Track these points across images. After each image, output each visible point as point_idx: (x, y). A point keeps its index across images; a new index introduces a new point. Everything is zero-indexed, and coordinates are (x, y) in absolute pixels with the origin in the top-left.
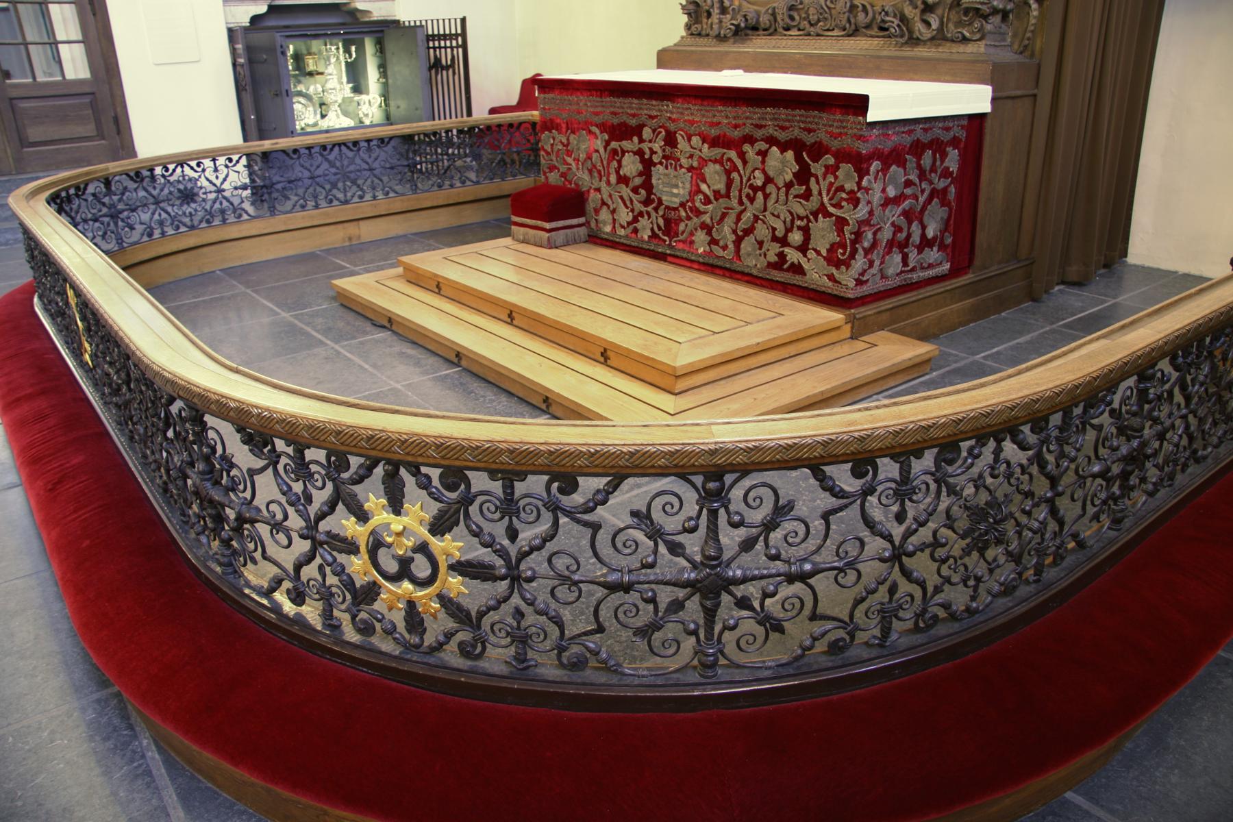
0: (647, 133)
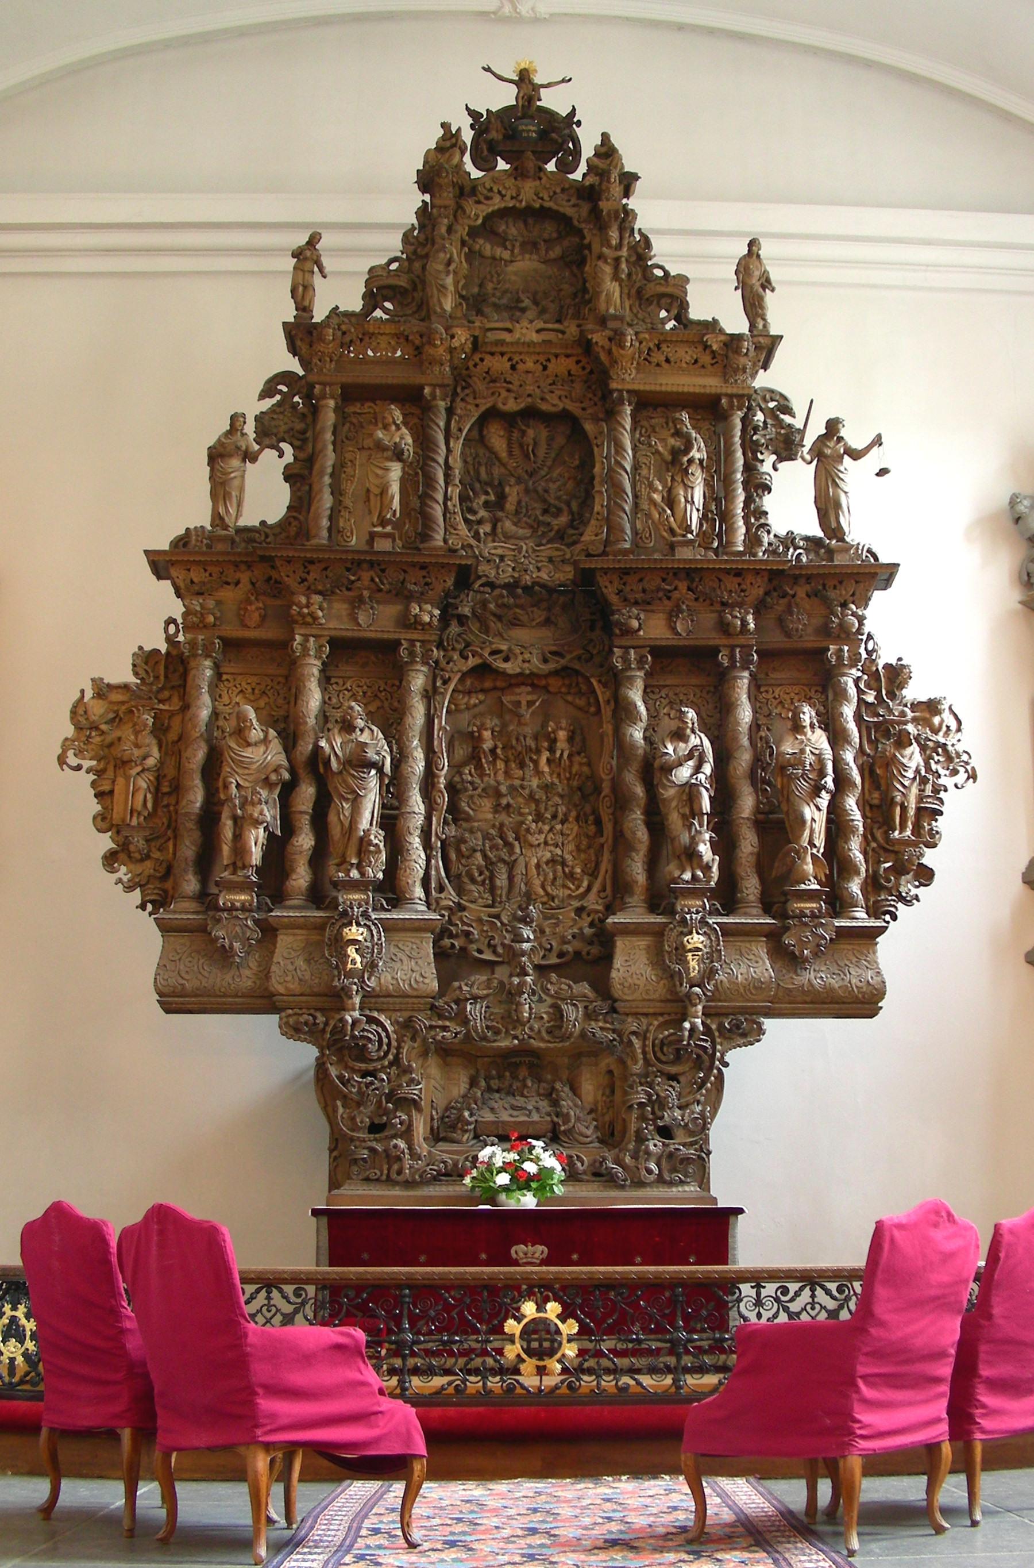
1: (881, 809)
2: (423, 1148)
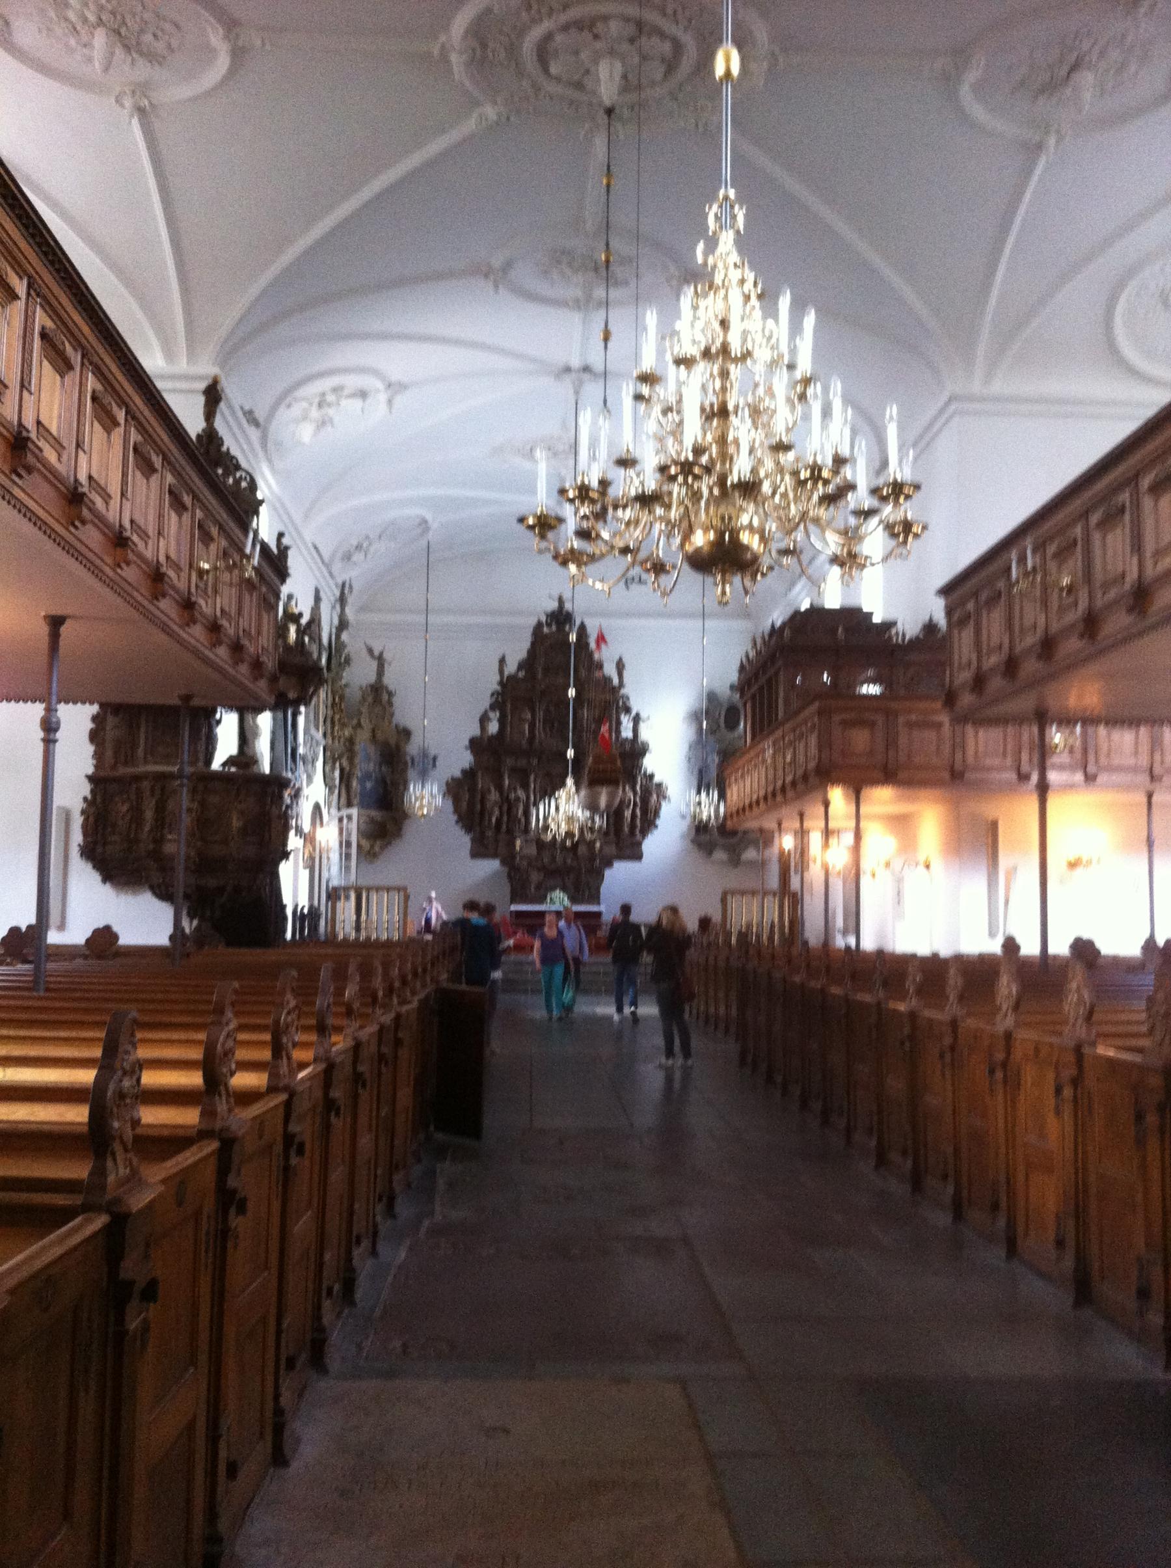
1: (645, 811)
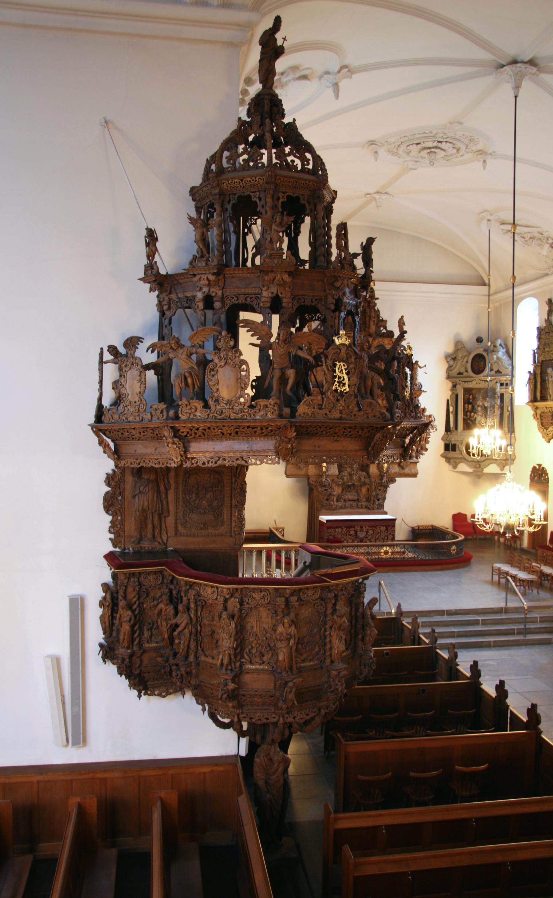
0: (356, 527)
2: (336, 503)
